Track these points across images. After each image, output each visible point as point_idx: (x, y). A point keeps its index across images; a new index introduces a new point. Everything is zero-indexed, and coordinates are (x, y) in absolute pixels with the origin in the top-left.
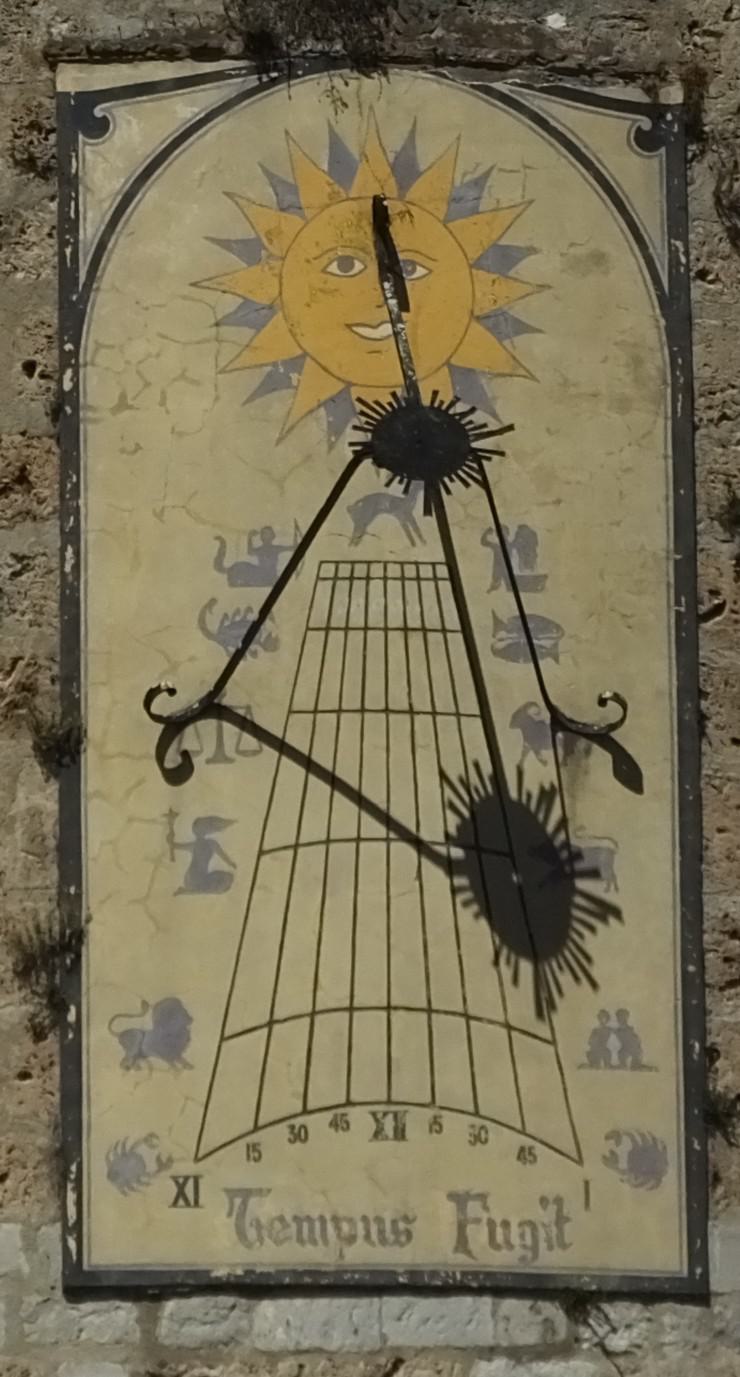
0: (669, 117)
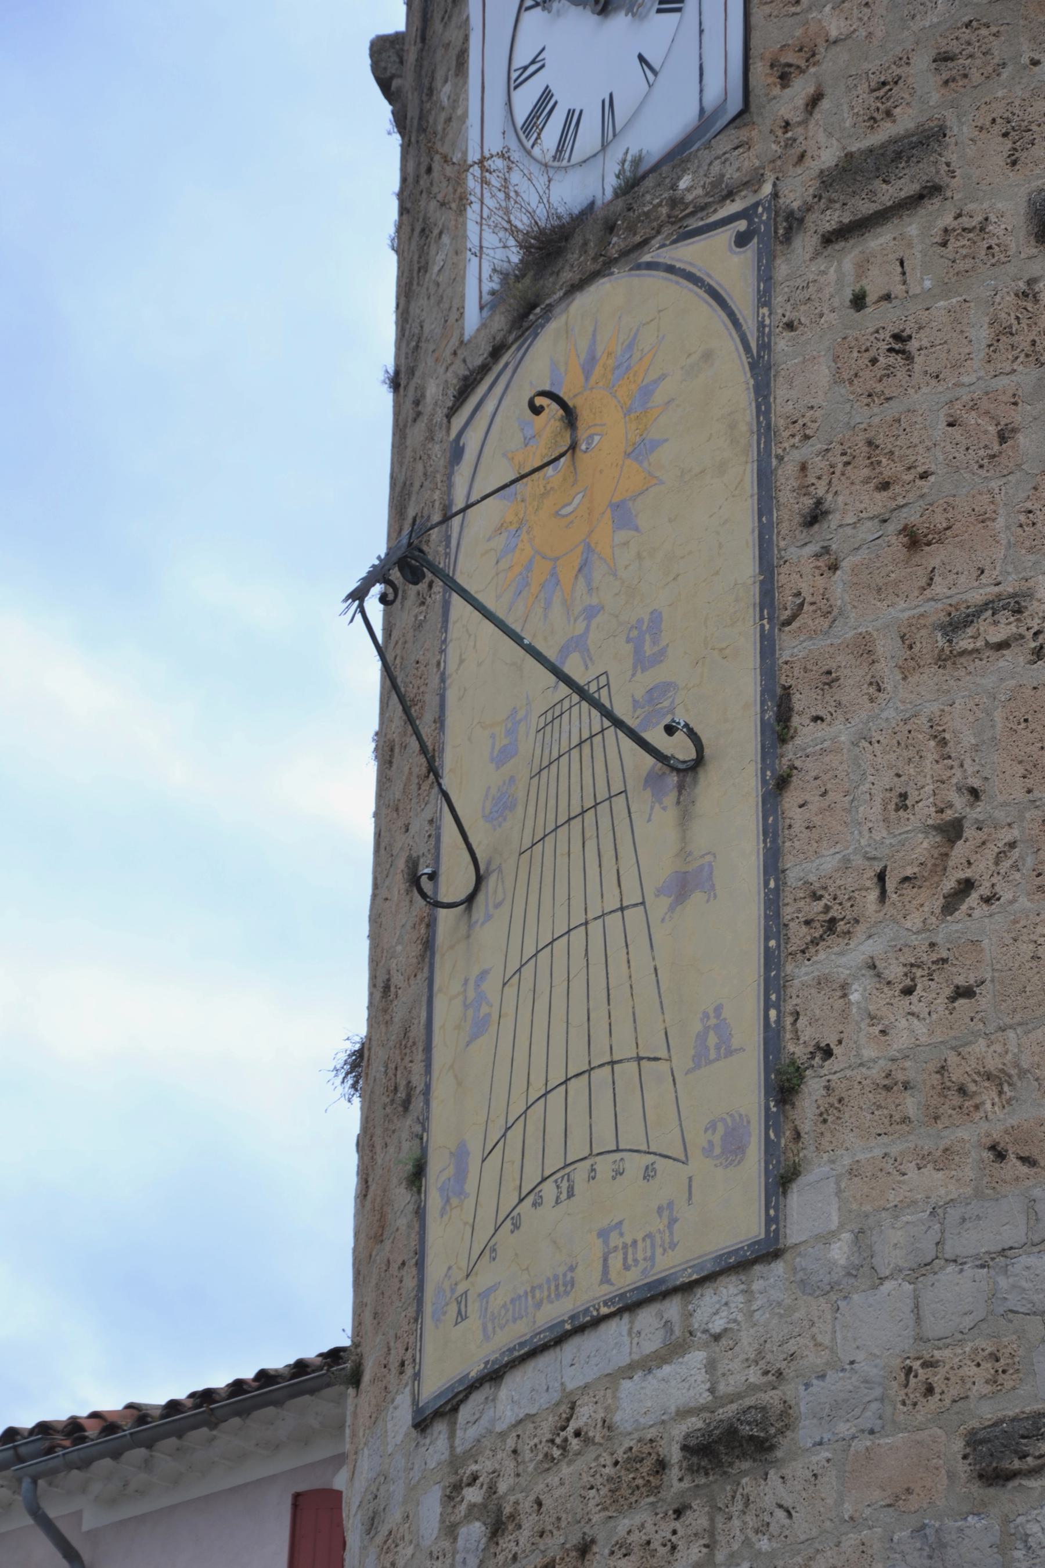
0: (760, 210)
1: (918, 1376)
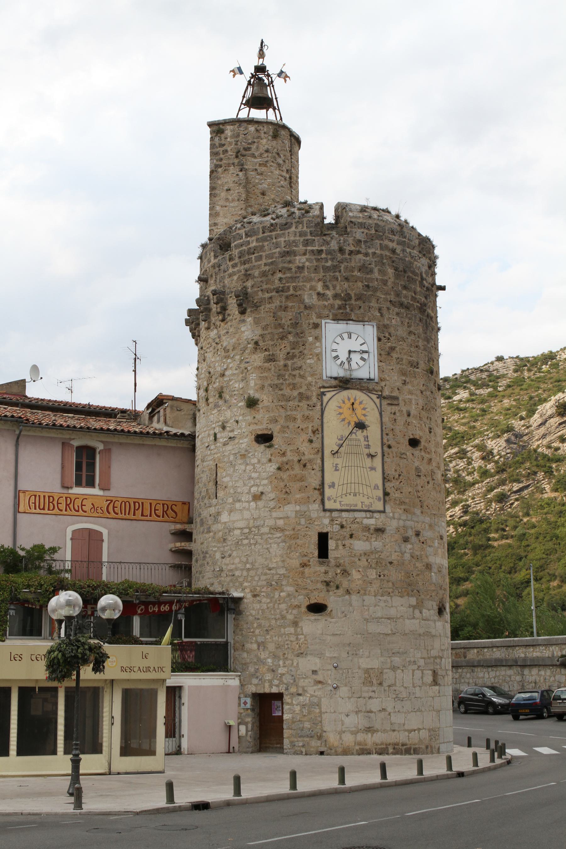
1: (398, 530)
